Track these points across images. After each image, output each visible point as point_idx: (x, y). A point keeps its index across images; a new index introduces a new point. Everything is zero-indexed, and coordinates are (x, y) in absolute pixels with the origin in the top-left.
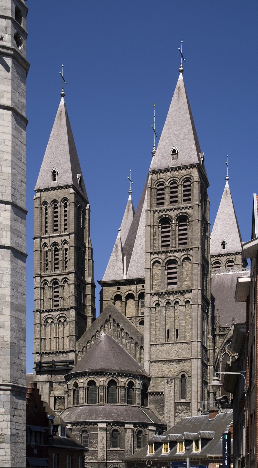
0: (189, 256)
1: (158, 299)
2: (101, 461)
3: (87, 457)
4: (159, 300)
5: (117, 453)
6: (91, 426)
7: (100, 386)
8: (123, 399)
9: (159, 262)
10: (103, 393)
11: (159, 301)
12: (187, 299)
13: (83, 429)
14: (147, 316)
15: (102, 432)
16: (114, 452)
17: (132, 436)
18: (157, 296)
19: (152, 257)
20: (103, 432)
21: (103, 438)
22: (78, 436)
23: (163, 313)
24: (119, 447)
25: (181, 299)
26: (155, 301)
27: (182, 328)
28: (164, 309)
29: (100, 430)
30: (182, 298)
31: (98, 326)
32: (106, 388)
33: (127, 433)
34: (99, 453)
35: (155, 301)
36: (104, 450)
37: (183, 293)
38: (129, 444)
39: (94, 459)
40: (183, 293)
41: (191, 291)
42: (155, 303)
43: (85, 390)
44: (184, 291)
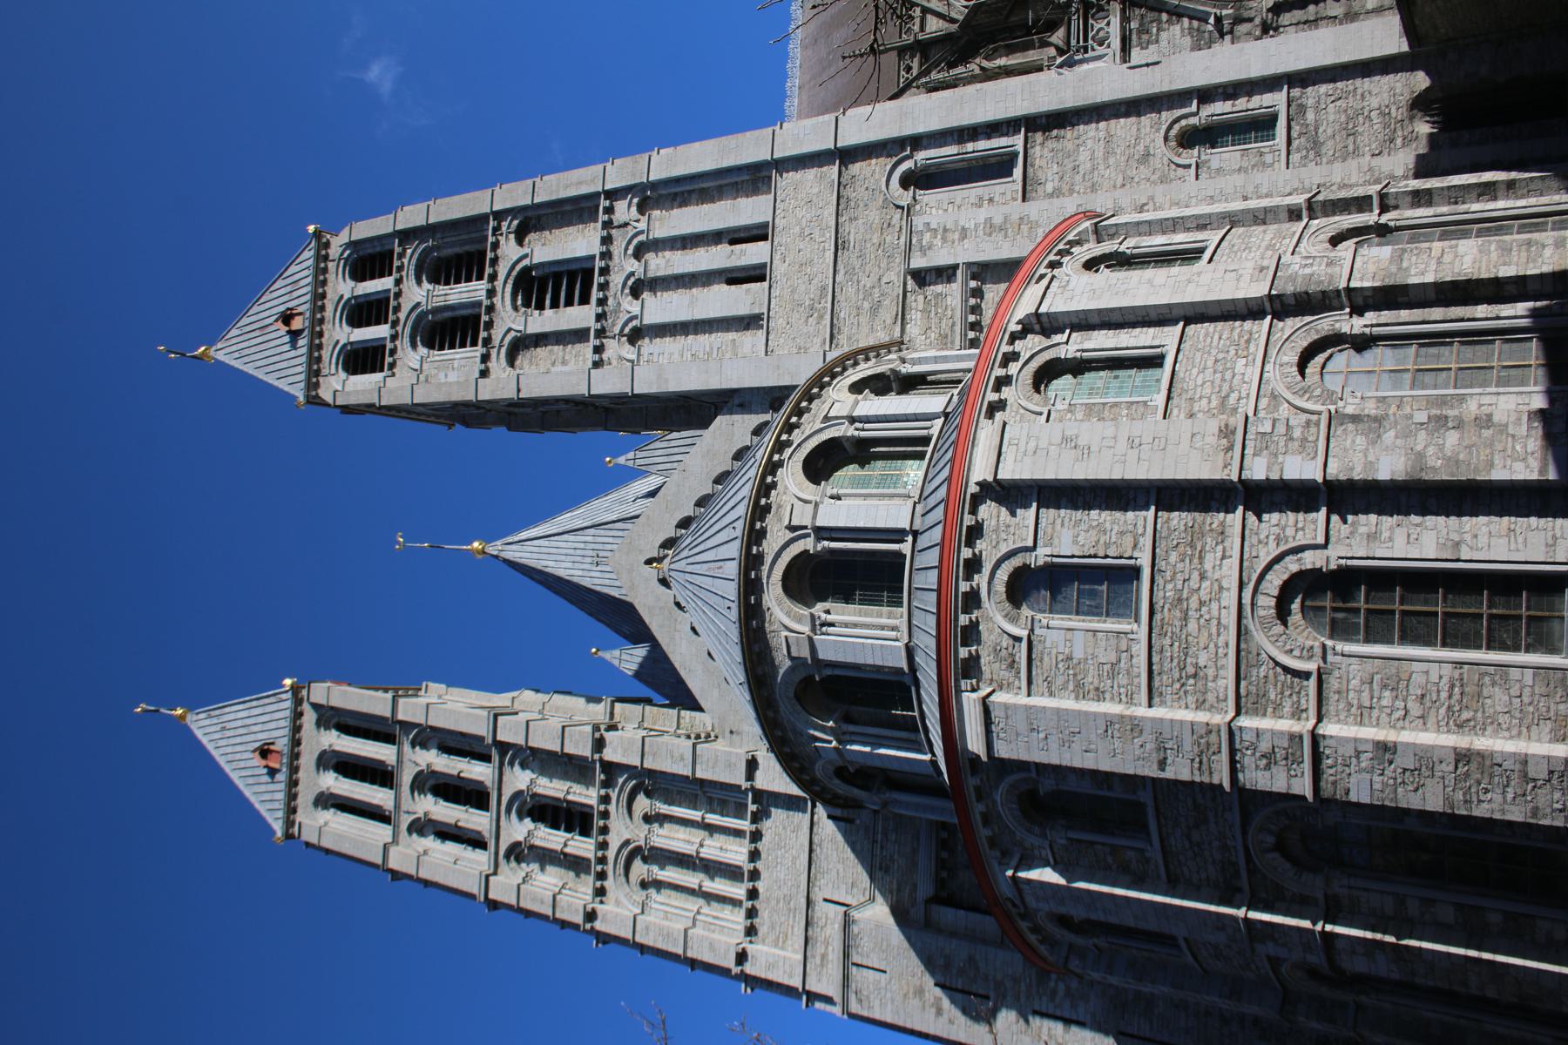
1: (614, 338)
4: (617, 332)
11: (621, 334)
12: (634, 209)
43: (831, 629)
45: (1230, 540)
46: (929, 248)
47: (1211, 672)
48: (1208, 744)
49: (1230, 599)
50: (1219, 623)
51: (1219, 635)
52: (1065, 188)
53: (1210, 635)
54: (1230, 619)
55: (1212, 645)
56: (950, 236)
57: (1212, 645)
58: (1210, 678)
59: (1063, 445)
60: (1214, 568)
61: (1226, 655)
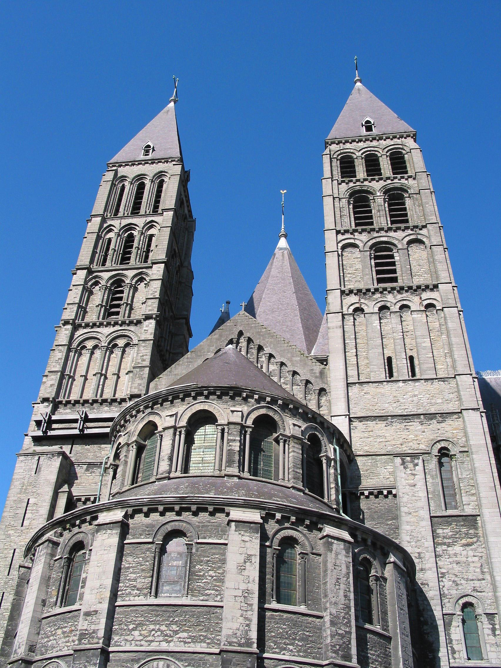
0: (419, 237)
2: (239, 649)
3: (176, 632)
5: (295, 624)
6: (204, 516)
7: (229, 423)
8: (298, 471)
9: (354, 246)
10: (238, 444)
13: (169, 528)
14: (337, 328)
15: (244, 538)
16: (287, 619)
17: (348, 567)
18: (355, 294)
19: (340, 237)
20: (247, 539)
21: (248, 558)
22: (148, 550)
23: (374, 325)
24: (305, 602)
25: (414, 302)
26: (352, 305)
27: (424, 351)
28: (376, 317)
29: (236, 531)
30: (416, 299)
31: (208, 352)
32: (248, 433)
33: (333, 552)
34: (226, 613)
35: (352, 305)
36: (251, 605)
37: (418, 289)
38: (341, 593)
39: (202, 641)
40: (418, 289)
41: (436, 286)
42: (352, 308)
43: (177, 437)
44: (419, 287)
45: (193, 646)
46: (404, 468)
47: (130, 638)
48: (93, 637)
49: (164, 646)
50: (152, 641)
51: (146, 641)
52: (439, 540)
53: (147, 636)
54: (154, 647)
55: (141, 638)
56: (412, 477)
57: (141, 638)
58: (126, 637)
59: (247, 556)
60: (180, 638)
61: (137, 645)
